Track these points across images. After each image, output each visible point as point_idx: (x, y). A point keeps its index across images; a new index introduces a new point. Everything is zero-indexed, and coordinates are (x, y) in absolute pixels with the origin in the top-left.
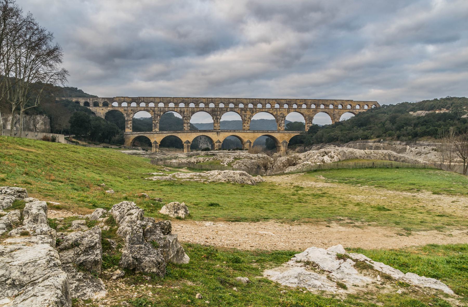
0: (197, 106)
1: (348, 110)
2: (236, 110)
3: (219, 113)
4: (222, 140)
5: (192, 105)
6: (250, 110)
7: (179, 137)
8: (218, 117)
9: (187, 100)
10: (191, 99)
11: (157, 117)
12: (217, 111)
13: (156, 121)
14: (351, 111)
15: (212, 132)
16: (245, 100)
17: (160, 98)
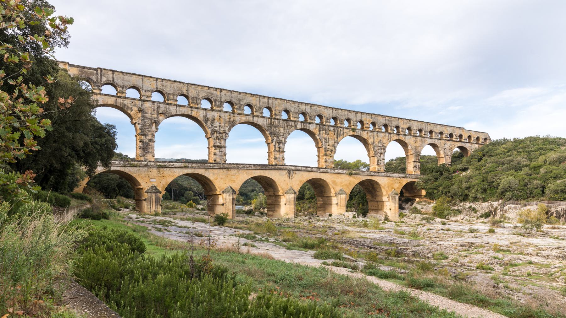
0: (240, 112)
1: (460, 144)
2: (312, 128)
3: (282, 130)
4: (297, 188)
5: (227, 107)
6: (334, 131)
7: (211, 178)
8: (281, 138)
9: (218, 93)
10: (228, 94)
11: (151, 125)
12: (279, 126)
13: (146, 135)
14: (463, 145)
15: (280, 169)
16: (326, 110)
17: (157, 79)
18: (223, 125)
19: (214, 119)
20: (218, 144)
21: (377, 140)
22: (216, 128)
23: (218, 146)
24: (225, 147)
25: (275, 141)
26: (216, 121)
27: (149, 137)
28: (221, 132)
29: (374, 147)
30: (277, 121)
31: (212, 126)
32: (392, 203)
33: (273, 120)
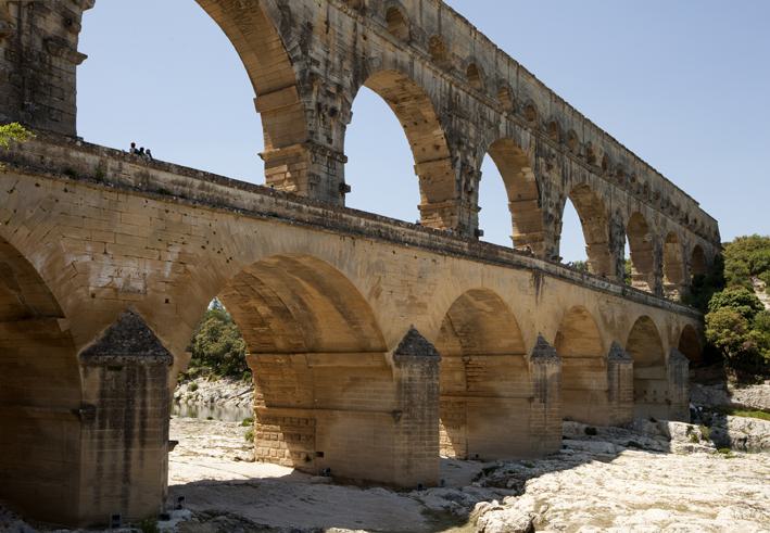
3: (472, 132)
18: (337, 60)
19: (309, 27)
20: (322, 140)
21: (615, 205)
22: (314, 68)
23: (324, 150)
24: (344, 159)
25: (459, 164)
26: (316, 37)
27: (51, 25)
28: (333, 90)
29: (610, 226)
30: (461, 92)
31: (305, 53)
32: (672, 387)
33: (454, 88)
